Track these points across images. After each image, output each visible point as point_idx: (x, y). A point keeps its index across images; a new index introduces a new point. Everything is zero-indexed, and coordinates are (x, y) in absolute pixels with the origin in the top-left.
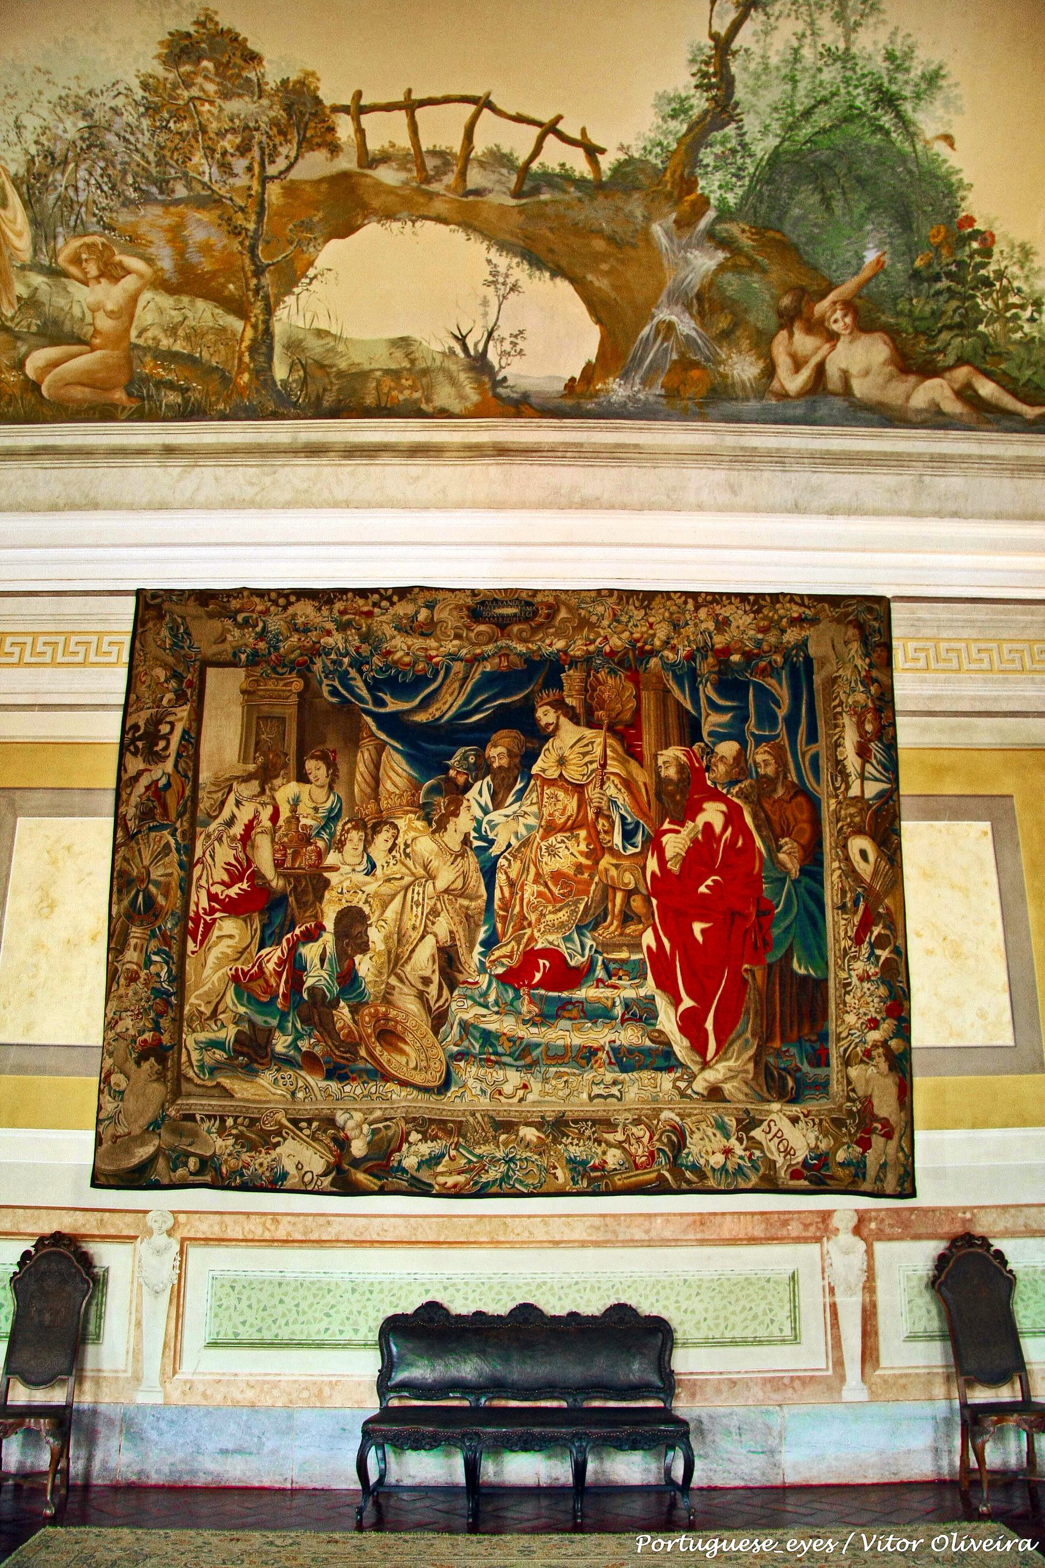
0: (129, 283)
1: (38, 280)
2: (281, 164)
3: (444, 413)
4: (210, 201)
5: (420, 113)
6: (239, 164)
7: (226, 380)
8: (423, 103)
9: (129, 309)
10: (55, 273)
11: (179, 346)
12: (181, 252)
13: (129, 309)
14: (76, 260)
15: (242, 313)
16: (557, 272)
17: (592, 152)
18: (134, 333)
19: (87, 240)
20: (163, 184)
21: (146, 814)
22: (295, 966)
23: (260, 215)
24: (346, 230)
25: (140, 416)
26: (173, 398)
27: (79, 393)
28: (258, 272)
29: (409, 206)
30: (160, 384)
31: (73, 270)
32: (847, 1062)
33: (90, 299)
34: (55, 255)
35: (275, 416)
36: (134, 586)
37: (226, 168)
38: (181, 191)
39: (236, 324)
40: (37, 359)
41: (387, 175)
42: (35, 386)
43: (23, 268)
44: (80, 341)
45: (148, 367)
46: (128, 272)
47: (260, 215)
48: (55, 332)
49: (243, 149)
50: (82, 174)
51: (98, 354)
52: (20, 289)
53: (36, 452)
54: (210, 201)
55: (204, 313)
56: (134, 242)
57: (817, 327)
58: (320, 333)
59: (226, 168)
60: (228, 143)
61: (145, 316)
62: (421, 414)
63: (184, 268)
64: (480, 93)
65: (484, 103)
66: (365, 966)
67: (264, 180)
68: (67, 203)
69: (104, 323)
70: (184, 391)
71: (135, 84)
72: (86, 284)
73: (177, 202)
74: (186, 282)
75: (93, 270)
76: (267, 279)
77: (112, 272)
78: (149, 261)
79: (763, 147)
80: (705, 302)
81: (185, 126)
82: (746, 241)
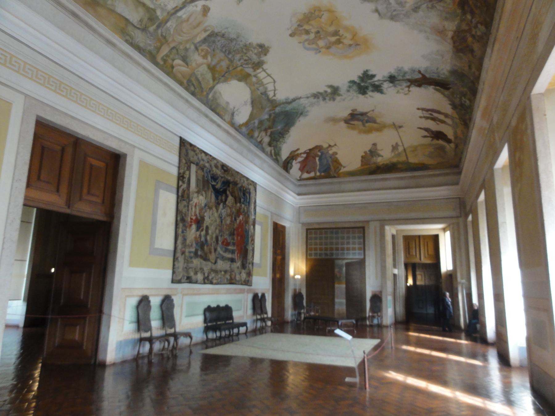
0: (205, 61)
1: (193, 47)
2: (247, 66)
3: (224, 120)
4: (231, 61)
5: (269, 77)
6: (242, 61)
7: (202, 91)
8: (271, 77)
9: (199, 66)
10: (197, 49)
11: (200, 79)
12: (218, 64)
13: (199, 66)
14: (202, 50)
15: (214, 79)
16: (253, 107)
17: (275, 96)
18: (196, 70)
19: (209, 49)
20: (230, 53)
21: (182, 196)
22: (200, 235)
23: (234, 69)
24: (240, 80)
25: (187, 89)
26: (192, 88)
27: (179, 76)
28: (223, 76)
29: (250, 85)
30: (193, 84)
31: (200, 51)
32: (249, 264)
33: (196, 58)
34: (201, 46)
35: (204, 104)
36: (180, 135)
37: (240, 60)
38: (230, 56)
39: (211, 82)
40: (178, 62)
41: (254, 79)
42: (173, 67)
43: (193, 43)
44: (187, 64)
45: (193, 79)
46: (207, 59)
47: (234, 69)
48: (185, 59)
49: (246, 60)
50: (223, 41)
51: (188, 69)
52: (188, 46)
53: (166, 84)
54: (231, 61)
55: (209, 76)
56: (213, 56)
57: (266, 133)
58: (220, 93)
59: (240, 60)
60: (245, 58)
61: (201, 69)
62: (222, 118)
63: (215, 66)
64: (276, 80)
65: (275, 82)
66: (208, 238)
67: (241, 66)
68: (214, 42)
69: (194, 65)
70: (195, 88)
71: (249, 42)
72: (199, 55)
73: (228, 57)
74: (212, 69)
75: (203, 53)
76: (223, 78)
77: (205, 57)
78: (212, 60)
79: (287, 109)
80: (261, 122)
81: (245, 51)
82: (272, 117)
